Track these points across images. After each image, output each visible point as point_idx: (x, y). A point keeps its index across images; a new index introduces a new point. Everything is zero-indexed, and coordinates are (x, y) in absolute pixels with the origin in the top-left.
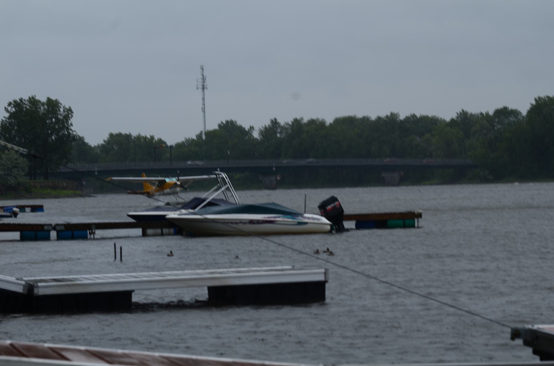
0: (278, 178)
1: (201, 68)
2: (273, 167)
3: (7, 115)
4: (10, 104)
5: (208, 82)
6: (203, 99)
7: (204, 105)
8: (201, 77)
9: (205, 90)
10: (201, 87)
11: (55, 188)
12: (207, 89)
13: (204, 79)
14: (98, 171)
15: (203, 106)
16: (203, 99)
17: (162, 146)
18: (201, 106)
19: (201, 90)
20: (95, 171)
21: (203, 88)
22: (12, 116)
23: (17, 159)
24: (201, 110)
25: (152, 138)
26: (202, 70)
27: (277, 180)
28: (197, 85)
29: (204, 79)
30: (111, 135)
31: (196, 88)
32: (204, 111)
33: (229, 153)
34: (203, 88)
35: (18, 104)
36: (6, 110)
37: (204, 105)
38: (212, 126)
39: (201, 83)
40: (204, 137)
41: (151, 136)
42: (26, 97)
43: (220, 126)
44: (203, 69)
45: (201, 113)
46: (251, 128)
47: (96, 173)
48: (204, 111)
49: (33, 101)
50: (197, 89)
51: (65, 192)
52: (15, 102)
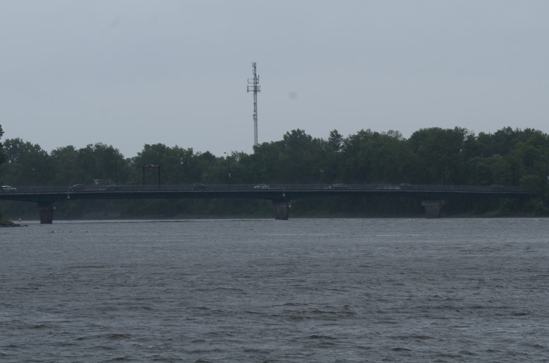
1: (253, 66)
2: (282, 193)
8: (253, 76)
9: (258, 93)
10: (253, 89)
13: (256, 79)
16: (255, 104)
17: (150, 167)
19: (253, 92)
21: (256, 91)
24: (252, 117)
25: (190, 151)
26: (253, 68)
27: (289, 208)
28: (248, 87)
29: (256, 79)
30: (147, 146)
31: (247, 91)
32: (256, 119)
33: (230, 176)
34: (256, 91)
39: (253, 85)
41: (189, 149)
43: (285, 137)
44: (255, 67)
47: (69, 197)
48: (256, 119)
50: (248, 91)
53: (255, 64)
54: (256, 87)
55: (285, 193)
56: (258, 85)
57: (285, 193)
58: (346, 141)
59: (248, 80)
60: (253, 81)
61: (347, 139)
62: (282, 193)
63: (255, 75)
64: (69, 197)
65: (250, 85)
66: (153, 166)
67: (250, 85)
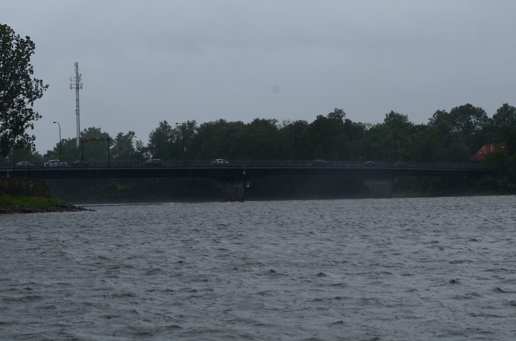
5: (82, 81)
6: (78, 100)
7: (78, 106)
8: (75, 75)
10: (75, 86)
12: (81, 88)
13: (78, 78)
16: (78, 100)
18: (75, 108)
19: (75, 89)
21: (78, 88)
24: (75, 112)
26: (75, 68)
28: (71, 84)
29: (78, 78)
32: (78, 114)
37: (78, 106)
39: (75, 83)
40: (78, 143)
44: (77, 67)
46: (130, 133)
48: (78, 114)
50: (71, 88)
53: (77, 63)
54: (78, 85)
56: (80, 83)
59: (71, 78)
60: (75, 79)
63: (77, 73)
65: (72, 83)
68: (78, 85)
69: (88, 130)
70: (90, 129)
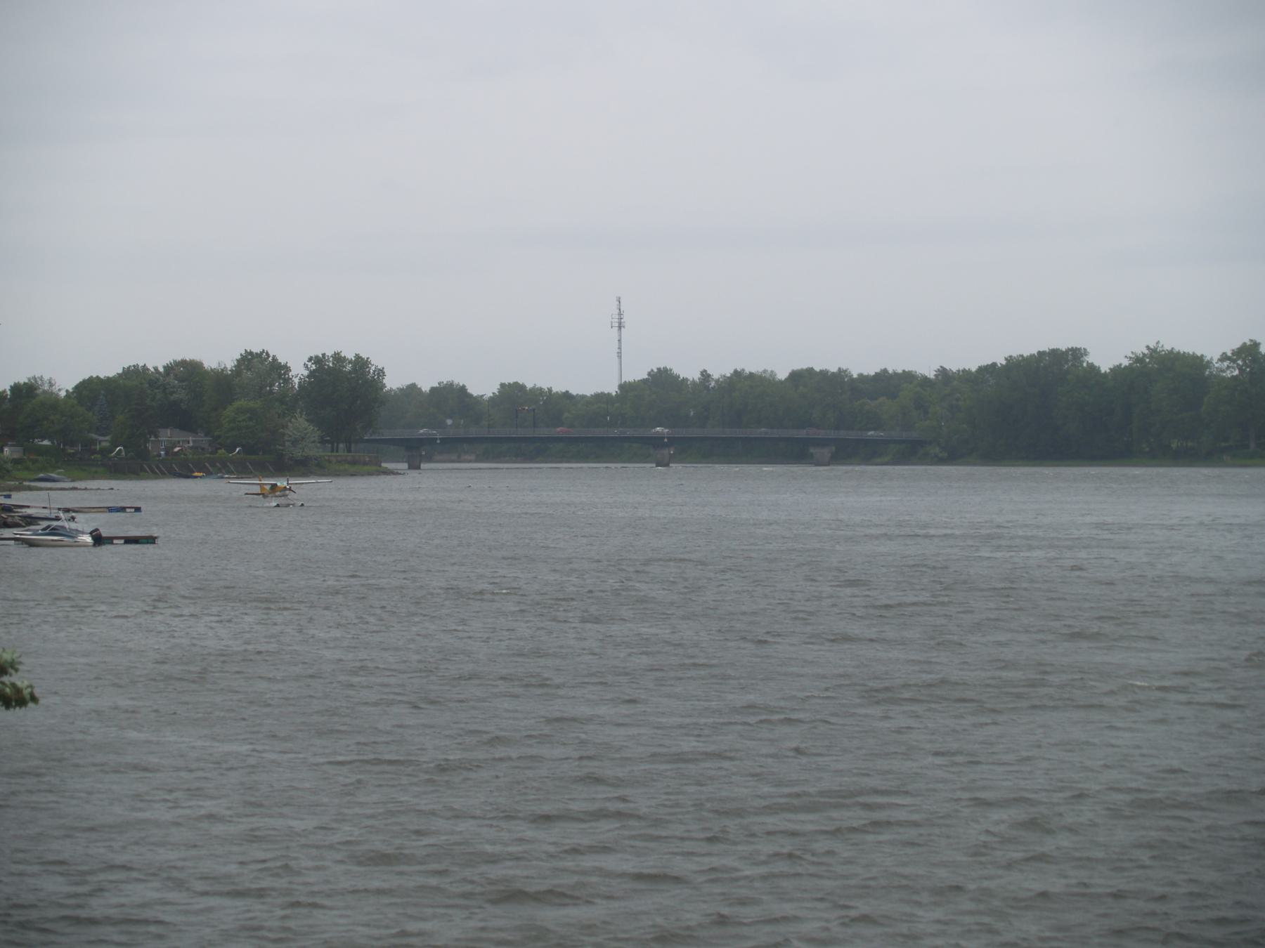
0: (672, 452)
2: (664, 438)
3: (306, 373)
4: (310, 360)
5: (625, 319)
6: (620, 341)
7: (620, 348)
8: (618, 311)
9: (622, 328)
11: (354, 462)
14: (440, 439)
15: (618, 350)
16: (620, 341)
17: (524, 409)
20: (437, 439)
21: (620, 326)
22: (312, 374)
23: (306, 429)
24: (616, 355)
26: (618, 303)
27: (670, 454)
28: (612, 322)
29: (620, 314)
30: (502, 385)
32: (620, 355)
35: (318, 360)
36: (306, 366)
37: (620, 348)
38: (637, 373)
39: (617, 320)
42: (329, 353)
43: (649, 374)
44: (620, 302)
45: (617, 359)
47: (438, 441)
48: (620, 355)
49: (338, 358)
50: (612, 327)
51: (367, 468)
52: (317, 357)
53: (619, 298)
54: (620, 323)
55: (668, 438)
56: (622, 320)
57: (668, 438)
58: (717, 381)
60: (617, 317)
61: (719, 379)
62: (664, 438)
63: (620, 310)
64: (438, 441)
65: (613, 320)
66: (527, 408)
67: (613, 320)
68: (620, 323)
69: (655, 370)
70: (659, 369)
